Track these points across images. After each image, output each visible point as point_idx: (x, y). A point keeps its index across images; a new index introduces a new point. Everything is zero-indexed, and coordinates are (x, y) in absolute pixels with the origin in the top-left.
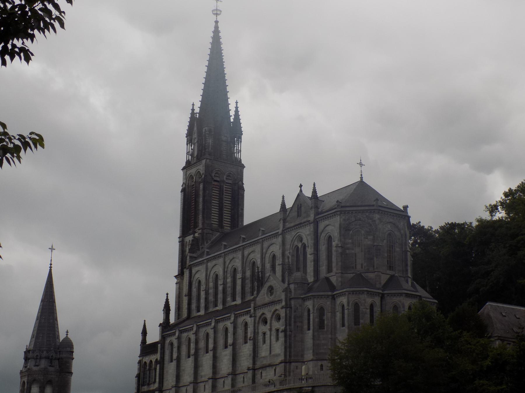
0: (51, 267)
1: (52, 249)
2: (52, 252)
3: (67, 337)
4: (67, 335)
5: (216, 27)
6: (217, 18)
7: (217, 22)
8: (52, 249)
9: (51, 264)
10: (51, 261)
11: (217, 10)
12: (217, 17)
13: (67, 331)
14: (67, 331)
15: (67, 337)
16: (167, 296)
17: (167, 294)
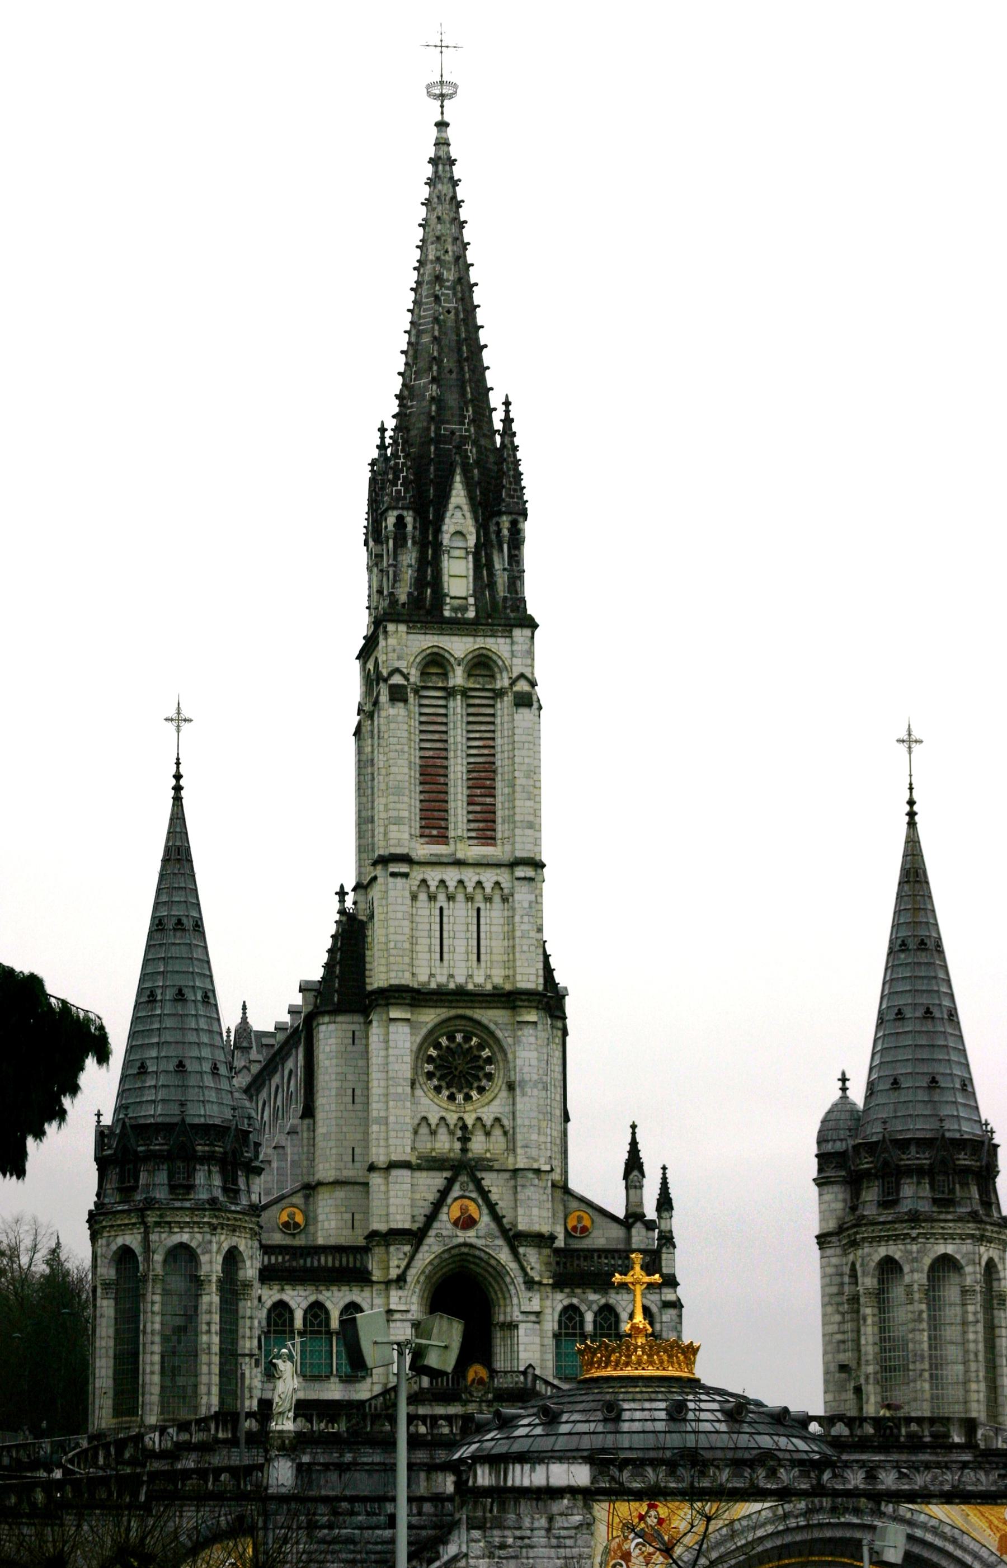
0: (912, 814)
1: (909, 741)
2: (910, 753)
3: (844, 1097)
4: (844, 1089)
5: (442, 143)
6: (442, 113)
7: (442, 125)
8: (909, 741)
9: (911, 803)
10: (911, 789)
11: (442, 83)
12: (442, 106)
13: (843, 1074)
14: (843, 1074)
15: (844, 1097)
16: (634, 1134)
17: (634, 1127)
